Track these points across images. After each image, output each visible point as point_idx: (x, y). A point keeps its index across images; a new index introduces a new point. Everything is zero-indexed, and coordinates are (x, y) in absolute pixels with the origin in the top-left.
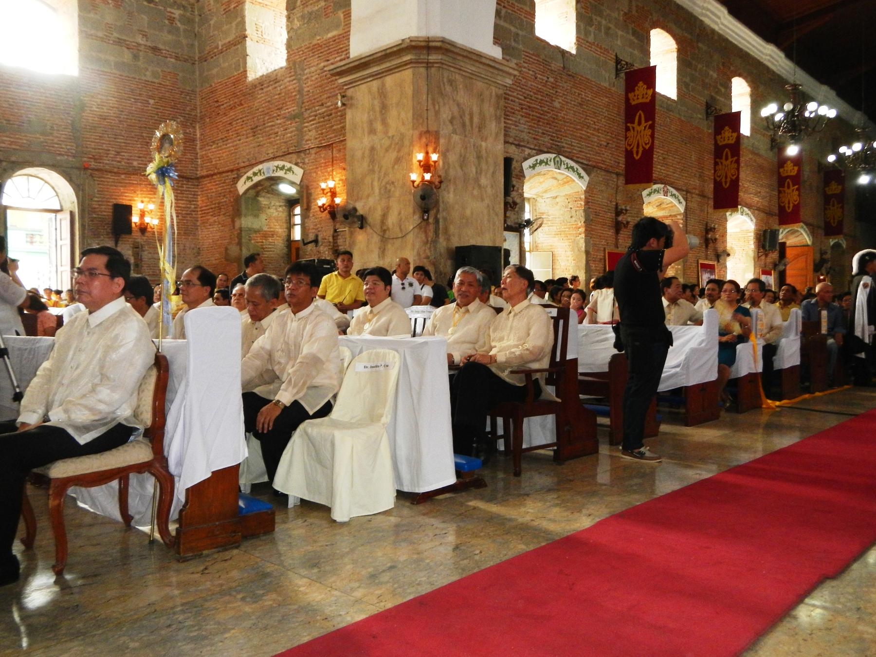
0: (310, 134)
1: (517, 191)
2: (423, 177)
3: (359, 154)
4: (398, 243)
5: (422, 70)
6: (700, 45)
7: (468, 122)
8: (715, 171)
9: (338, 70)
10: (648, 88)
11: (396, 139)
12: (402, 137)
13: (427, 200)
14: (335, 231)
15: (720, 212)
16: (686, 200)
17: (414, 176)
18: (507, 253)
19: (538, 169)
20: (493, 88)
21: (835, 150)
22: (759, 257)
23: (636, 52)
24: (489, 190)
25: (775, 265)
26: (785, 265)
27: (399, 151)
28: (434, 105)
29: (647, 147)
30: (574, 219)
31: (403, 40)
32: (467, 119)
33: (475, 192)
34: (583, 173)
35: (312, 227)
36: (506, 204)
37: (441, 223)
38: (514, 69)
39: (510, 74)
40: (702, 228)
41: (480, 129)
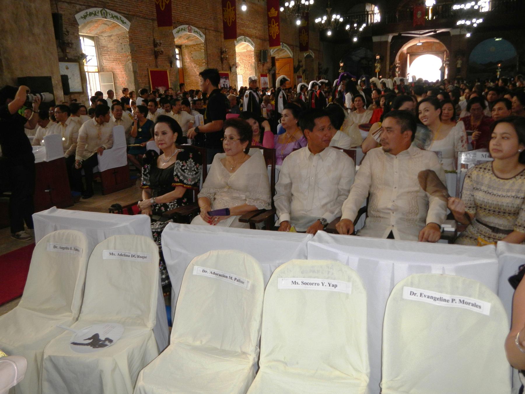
1: (73, 34)
8: (223, 15)
15: (228, 43)
16: (205, 34)
19: (89, 18)
21: (284, 6)
25: (269, 71)
33: (30, 39)
34: (125, 20)
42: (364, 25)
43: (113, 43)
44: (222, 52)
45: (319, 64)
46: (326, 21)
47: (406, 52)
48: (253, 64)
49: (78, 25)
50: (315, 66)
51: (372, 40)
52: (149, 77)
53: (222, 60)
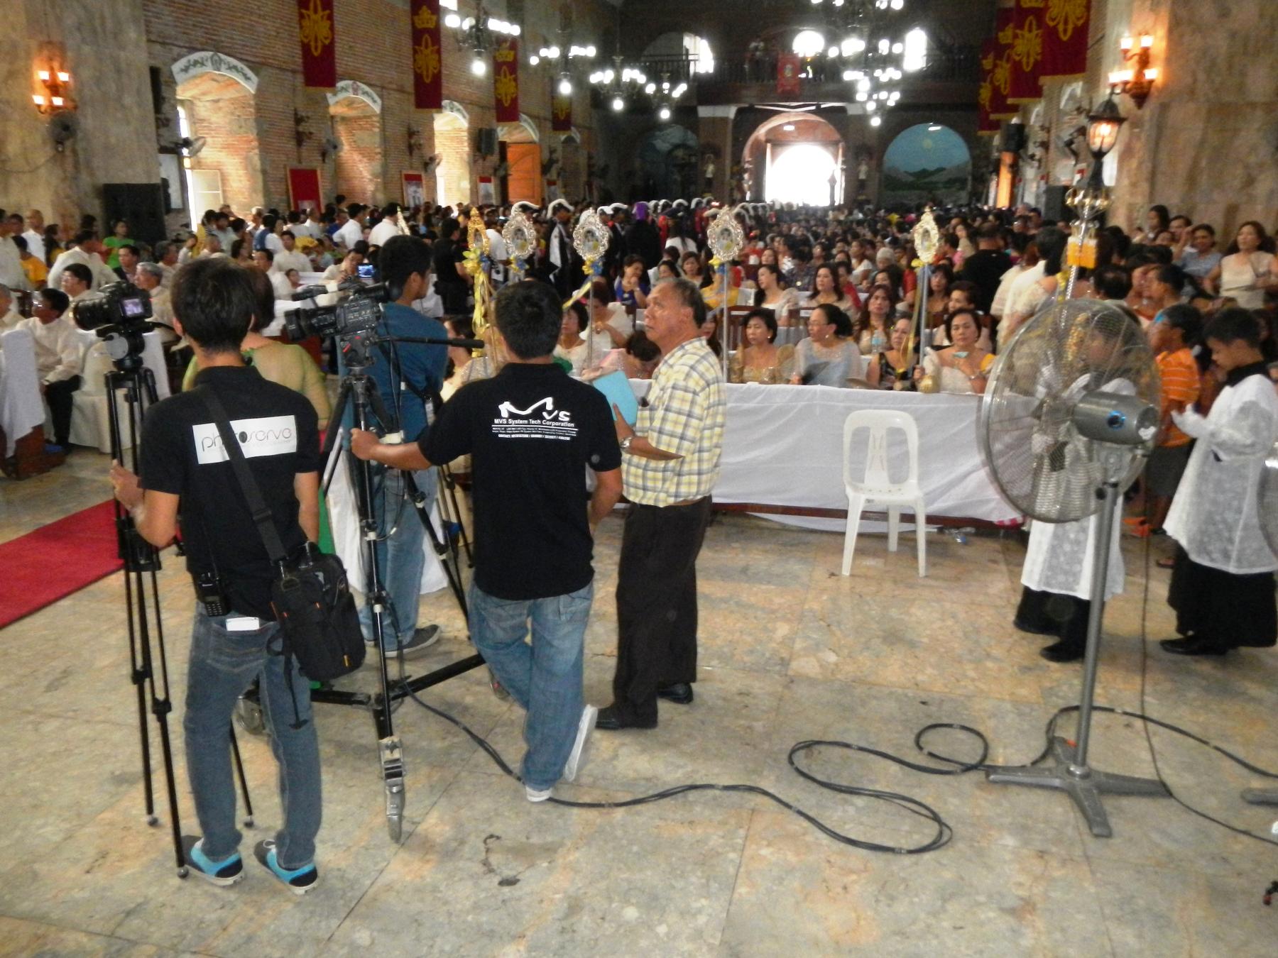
2: (51, 102)
4: (26, 178)
7: (99, 29)
8: (415, 60)
13: (63, 128)
15: (423, 113)
16: (381, 97)
17: (39, 99)
18: (165, 183)
19: (193, 71)
21: (537, 53)
22: (475, 162)
24: (136, 110)
25: (496, 170)
28: (53, 7)
29: (327, 42)
32: (97, 23)
36: (157, 120)
40: (404, 130)
41: (115, 36)
42: (682, 88)
43: (221, 114)
44: (411, 134)
45: (590, 157)
47: (763, 138)
48: (465, 157)
49: (175, 83)
50: (582, 160)
53: (411, 148)
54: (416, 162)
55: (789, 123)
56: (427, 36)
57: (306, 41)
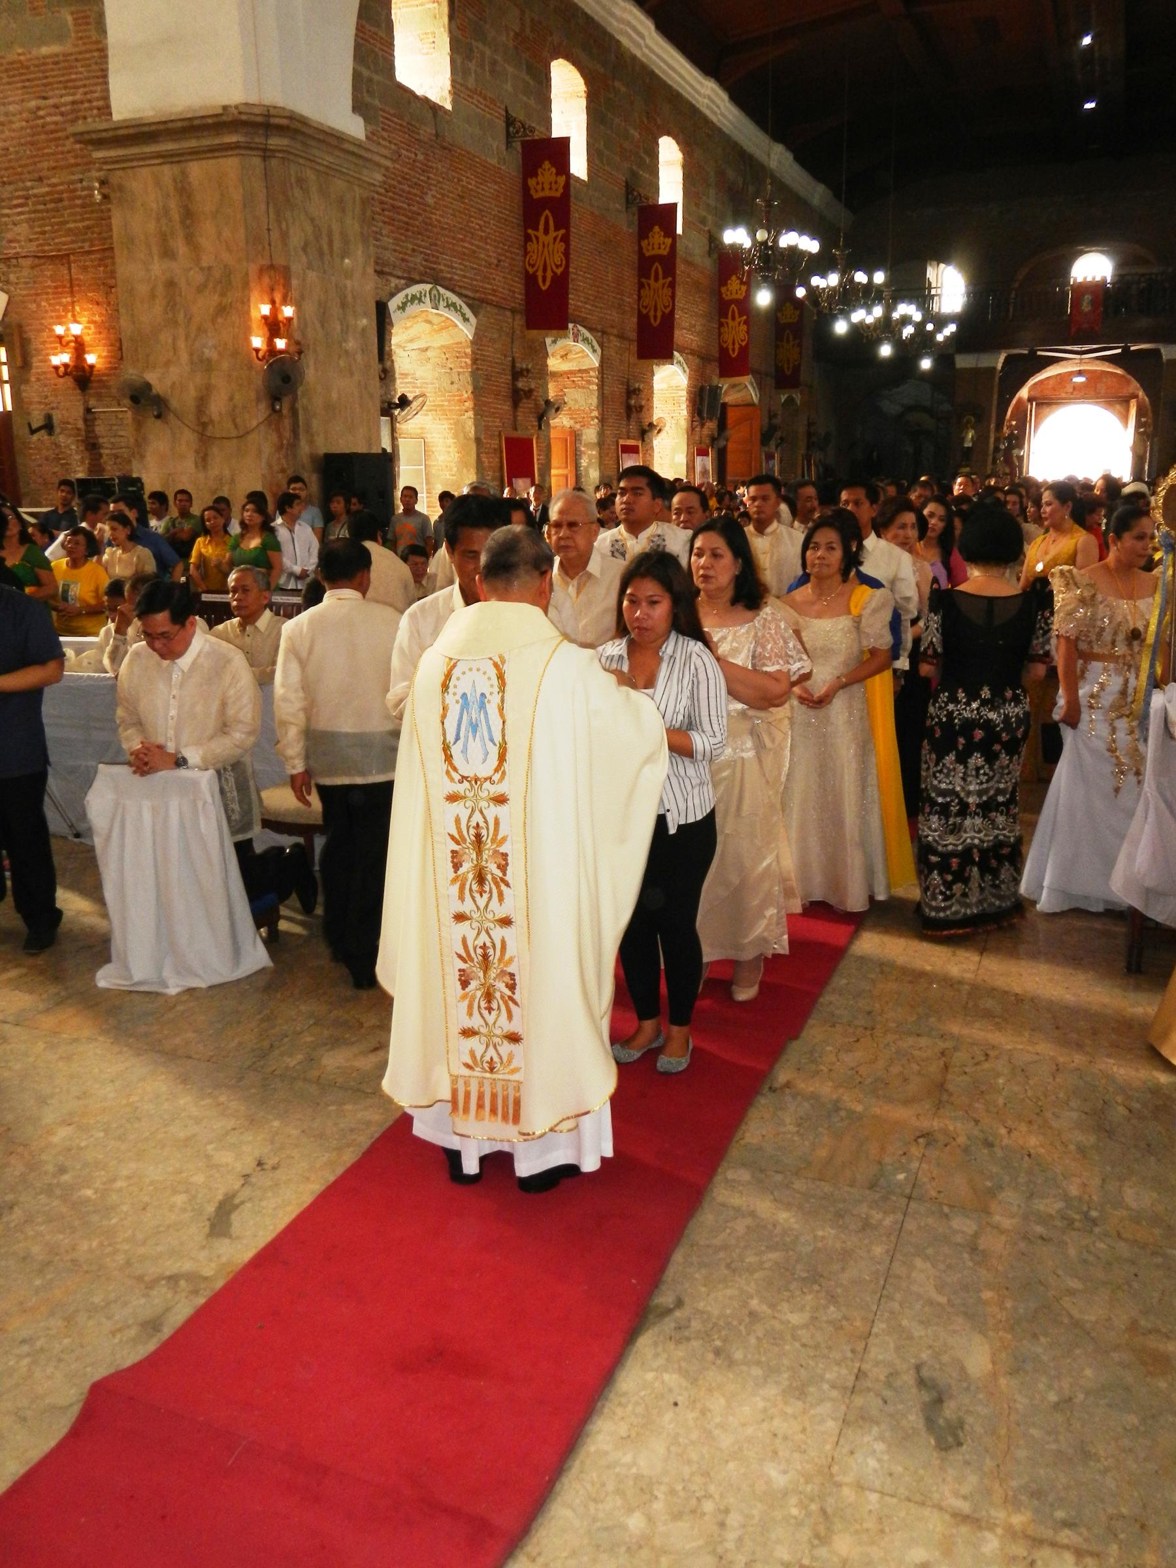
0: (17, 229)
3: (143, 289)
5: (256, 161)
6: (617, 84)
7: (325, 247)
9: (94, 136)
10: (558, 174)
11: (217, 274)
12: (228, 272)
13: (282, 379)
14: (88, 410)
16: (601, 345)
17: (257, 342)
19: (410, 309)
20: (356, 189)
21: (806, 283)
23: (532, 102)
24: (359, 357)
25: (713, 440)
26: (727, 440)
27: (223, 295)
28: (279, 222)
29: (559, 271)
30: (456, 386)
31: (225, 108)
35: (36, 399)
37: (301, 417)
38: (386, 157)
39: (378, 165)
43: (429, 366)
45: (810, 424)
46: (878, 320)
50: (802, 429)
51: (953, 363)
52: (501, 452)
53: (629, 410)
54: (633, 427)
55: (1080, 373)
56: (657, 264)
57: (531, 270)
